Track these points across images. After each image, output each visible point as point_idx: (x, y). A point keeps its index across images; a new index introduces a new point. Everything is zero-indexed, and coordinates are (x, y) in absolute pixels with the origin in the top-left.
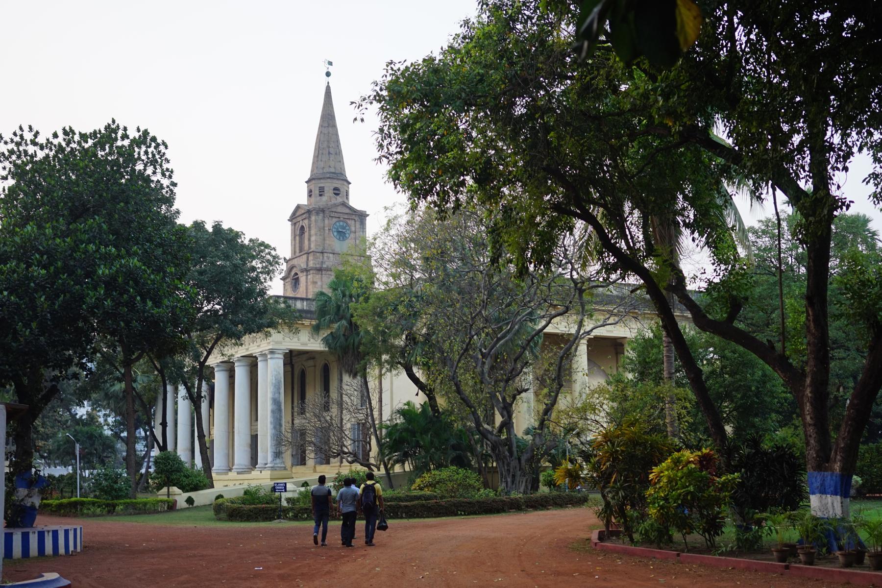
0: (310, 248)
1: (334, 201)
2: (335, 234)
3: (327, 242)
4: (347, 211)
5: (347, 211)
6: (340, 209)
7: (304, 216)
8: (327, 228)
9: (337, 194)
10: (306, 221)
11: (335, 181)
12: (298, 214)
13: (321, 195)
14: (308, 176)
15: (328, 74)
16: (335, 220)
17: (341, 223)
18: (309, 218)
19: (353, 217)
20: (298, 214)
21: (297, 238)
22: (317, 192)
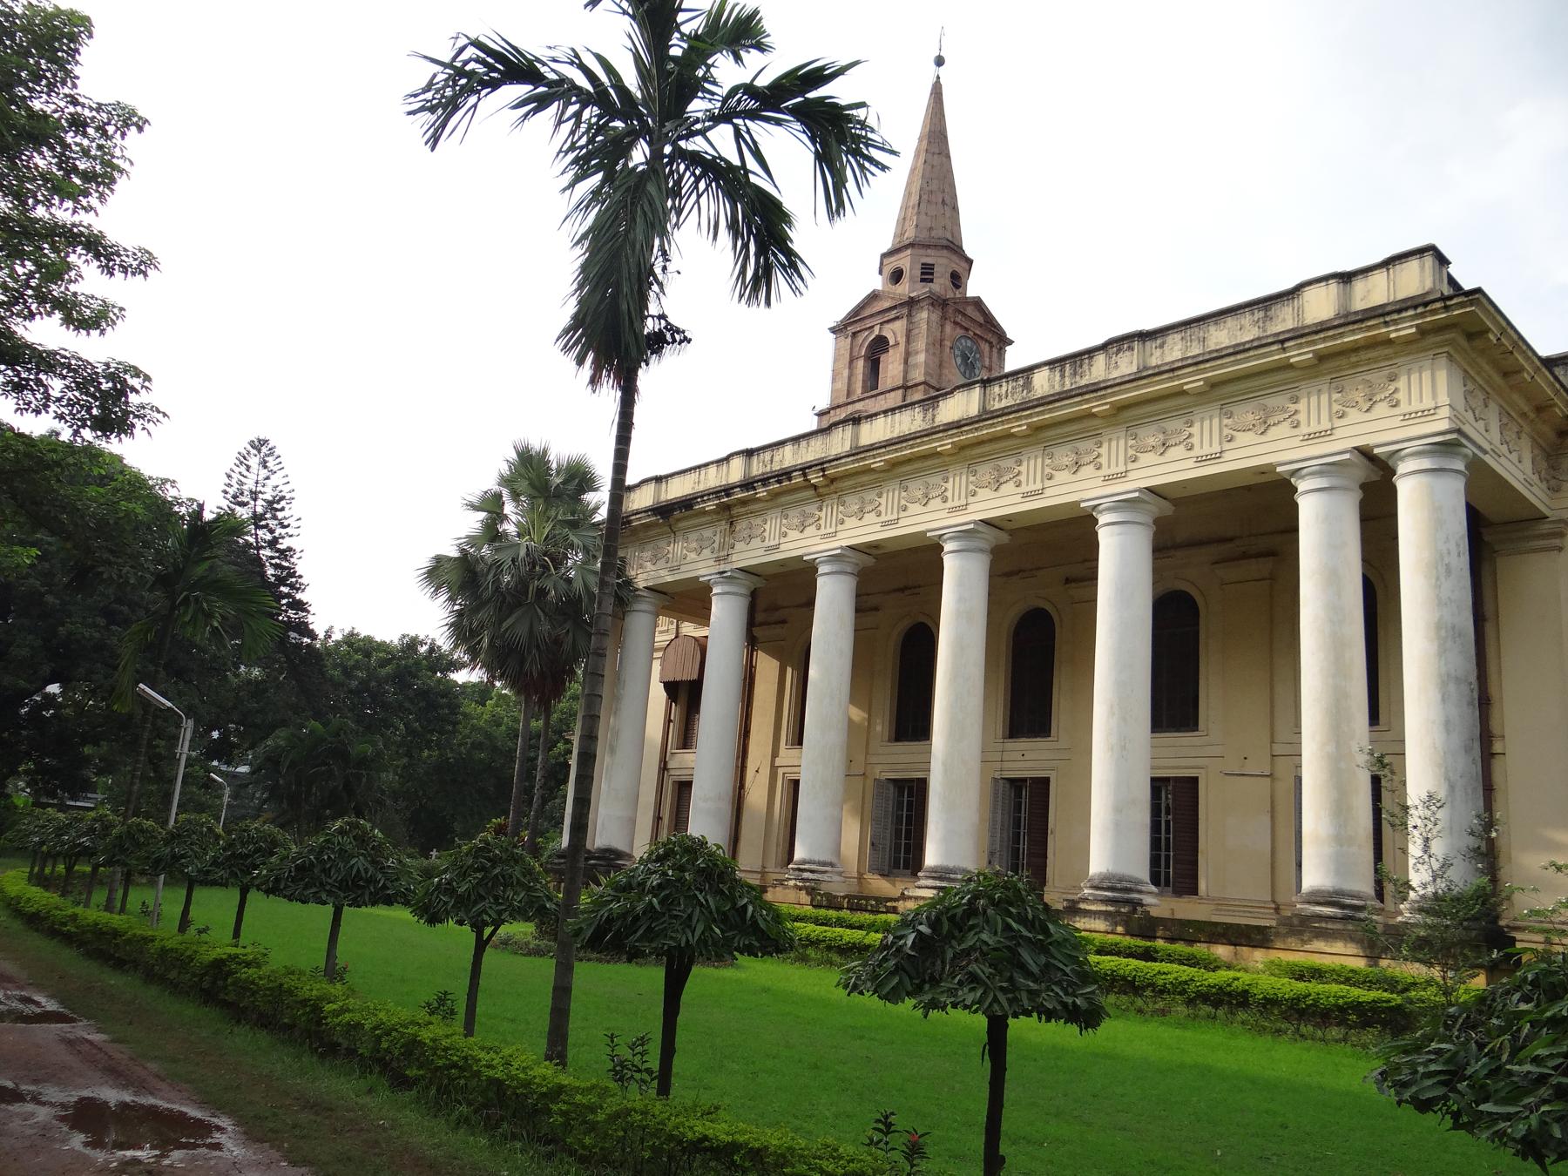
0: (905, 378)
1: (950, 295)
2: (959, 360)
3: (945, 371)
4: (981, 320)
5: (981, 320)
6: (970, 311)
7: (893, 314)
8: (948, 343)
9: (957, 287)
10: (899, 326)
11: (954, 258)
12: (867, 312)
13: (922, 280)
14: (887, 246)
15: (940, 61)
16: (960, 332)
17: (969, 343)
18: (910, 315)
19: (989, 336)
20: (867, 312)
21: (860, 364)
22: (918, 272)
